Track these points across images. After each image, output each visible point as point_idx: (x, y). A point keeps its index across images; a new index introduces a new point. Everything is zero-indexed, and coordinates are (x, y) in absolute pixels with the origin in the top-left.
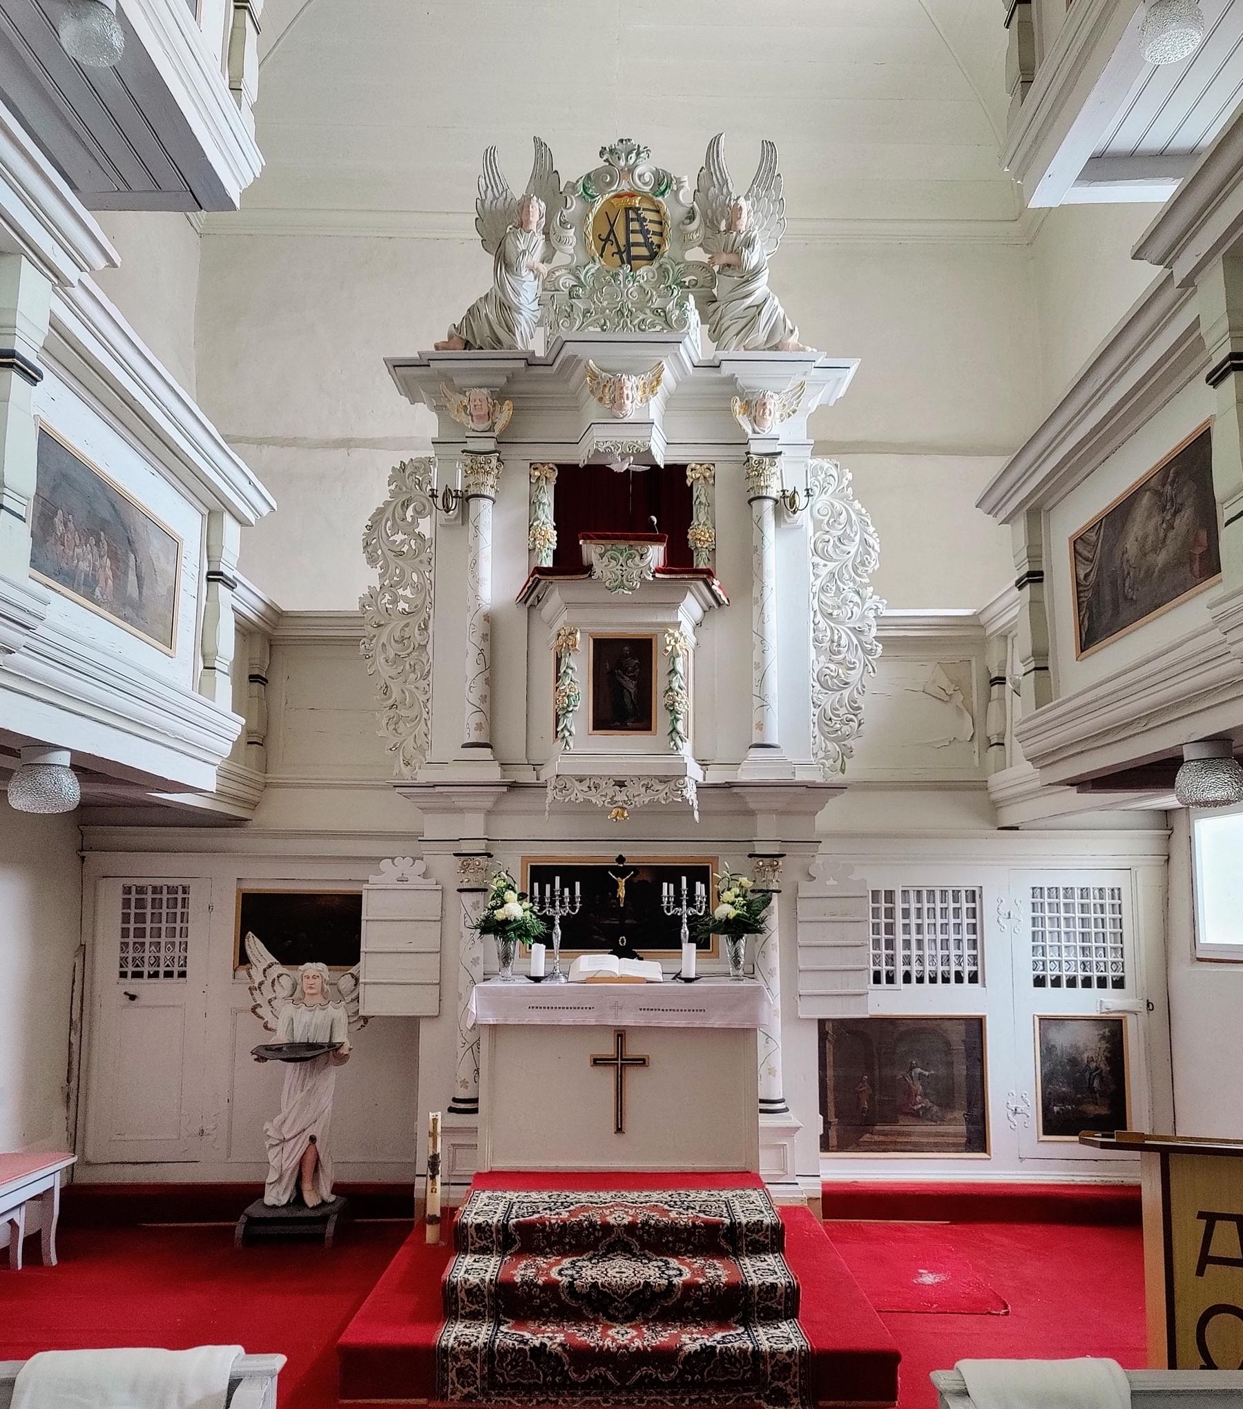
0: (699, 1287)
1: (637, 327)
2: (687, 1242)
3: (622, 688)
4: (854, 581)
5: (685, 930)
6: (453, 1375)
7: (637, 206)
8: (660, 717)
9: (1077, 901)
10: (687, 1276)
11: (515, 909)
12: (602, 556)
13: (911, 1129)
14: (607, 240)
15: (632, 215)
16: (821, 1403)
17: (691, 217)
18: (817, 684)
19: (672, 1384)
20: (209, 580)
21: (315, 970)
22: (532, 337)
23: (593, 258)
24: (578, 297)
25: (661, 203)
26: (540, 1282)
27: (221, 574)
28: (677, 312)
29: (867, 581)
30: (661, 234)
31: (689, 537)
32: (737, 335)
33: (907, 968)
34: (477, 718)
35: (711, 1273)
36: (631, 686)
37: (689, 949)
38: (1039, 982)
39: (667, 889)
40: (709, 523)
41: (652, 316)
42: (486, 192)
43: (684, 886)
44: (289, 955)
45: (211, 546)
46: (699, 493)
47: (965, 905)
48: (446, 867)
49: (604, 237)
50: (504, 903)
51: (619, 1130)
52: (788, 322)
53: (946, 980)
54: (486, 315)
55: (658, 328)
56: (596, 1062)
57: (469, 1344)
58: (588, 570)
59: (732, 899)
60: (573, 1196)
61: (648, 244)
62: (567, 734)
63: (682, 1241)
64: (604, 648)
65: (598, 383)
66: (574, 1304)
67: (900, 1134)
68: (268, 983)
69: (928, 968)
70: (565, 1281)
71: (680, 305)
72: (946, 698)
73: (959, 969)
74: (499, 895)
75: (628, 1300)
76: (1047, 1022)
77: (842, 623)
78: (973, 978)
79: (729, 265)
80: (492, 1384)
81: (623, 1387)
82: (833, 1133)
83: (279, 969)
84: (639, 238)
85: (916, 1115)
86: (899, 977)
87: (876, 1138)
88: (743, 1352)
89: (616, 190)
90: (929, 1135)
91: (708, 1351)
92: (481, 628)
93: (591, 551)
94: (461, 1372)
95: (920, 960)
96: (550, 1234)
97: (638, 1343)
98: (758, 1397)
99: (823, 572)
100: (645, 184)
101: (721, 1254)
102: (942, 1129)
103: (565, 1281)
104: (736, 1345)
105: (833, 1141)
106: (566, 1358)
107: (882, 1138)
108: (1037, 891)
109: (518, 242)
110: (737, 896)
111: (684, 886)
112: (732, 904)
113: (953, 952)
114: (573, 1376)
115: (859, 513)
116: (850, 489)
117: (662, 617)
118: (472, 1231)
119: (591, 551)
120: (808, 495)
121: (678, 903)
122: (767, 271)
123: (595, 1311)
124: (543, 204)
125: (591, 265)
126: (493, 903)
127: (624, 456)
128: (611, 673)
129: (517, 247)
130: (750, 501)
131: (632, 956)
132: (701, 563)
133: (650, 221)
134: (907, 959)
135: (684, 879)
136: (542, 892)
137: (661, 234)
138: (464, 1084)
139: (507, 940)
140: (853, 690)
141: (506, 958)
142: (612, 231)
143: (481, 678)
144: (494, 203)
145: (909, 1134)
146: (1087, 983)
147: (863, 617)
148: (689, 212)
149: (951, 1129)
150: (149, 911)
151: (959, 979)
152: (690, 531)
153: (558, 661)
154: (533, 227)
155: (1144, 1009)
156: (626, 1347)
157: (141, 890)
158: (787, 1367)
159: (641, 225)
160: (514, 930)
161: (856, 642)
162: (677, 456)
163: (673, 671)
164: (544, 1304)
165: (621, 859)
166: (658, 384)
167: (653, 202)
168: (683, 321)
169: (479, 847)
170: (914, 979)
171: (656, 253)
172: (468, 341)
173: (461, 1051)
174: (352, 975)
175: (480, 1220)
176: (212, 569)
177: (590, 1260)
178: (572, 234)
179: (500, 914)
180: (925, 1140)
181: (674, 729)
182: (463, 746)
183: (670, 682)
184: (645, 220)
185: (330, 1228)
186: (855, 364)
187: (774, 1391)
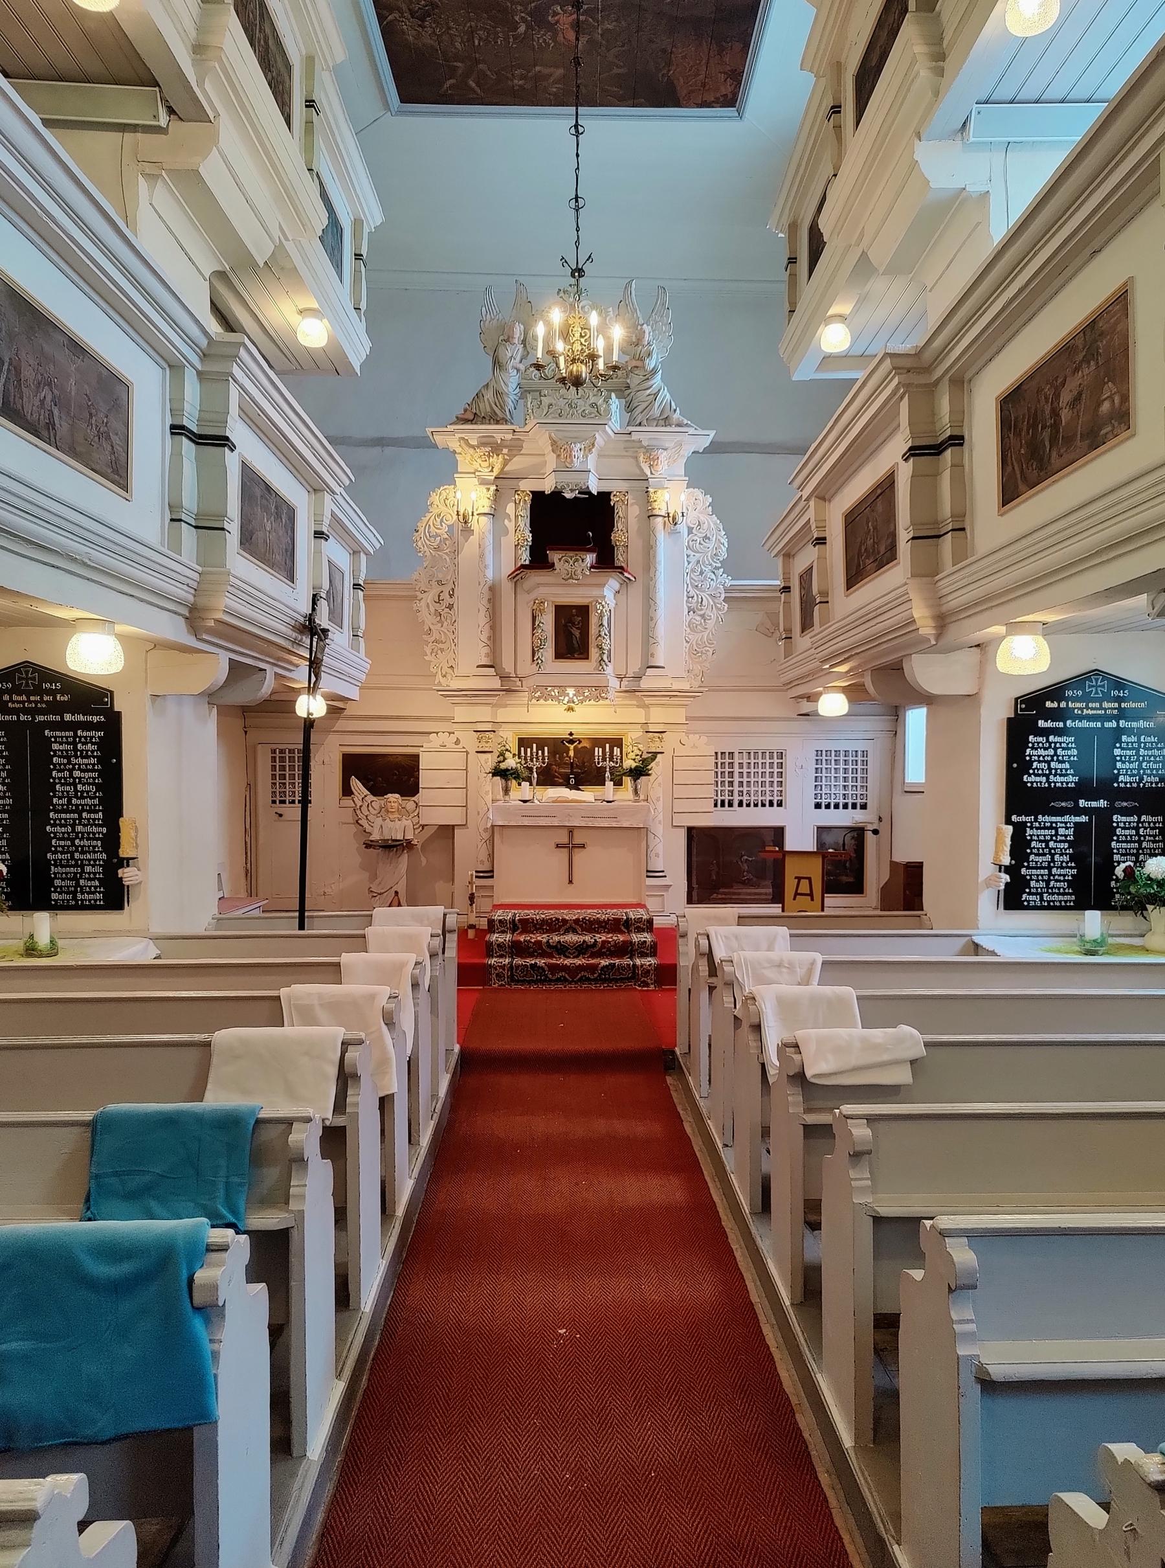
0: (609, 942)
2: (605, 928)
3: (570, 635)
5: (608, 774)
6: (494, 976)
8: (594, 652)
9: (842, 758)
10: (604, 938)
11: (511, 763)
12: (560, 560)
13: (740, 891)
18: (688, 629)
19: (595, 980)
20: (354, 588)
21: (393, 797)
22: (515, 409)
26: (533, 941)
27: (360, 585)
29: (720, 565)
31: (612, 538)
32: (642, 412)
33: (741, 798)
34: (486, 650)
35: (615, 938)
36: (577, 633)
37: (609, 784)
38: (818, 806)
39: (598, 752)
42: (486, 316)
43: (607, 750)
44: (377, 790)
45: (355, 573)
46: (620, 511)
47: (776, 761)
48: (470, 741)
50: (505, 759)
51: (571, 882)
53: (763, 805)
54: (488, 399)
55: (593, 415)
56: (558, 846)
58: (551, 566)
59: (634, 757)
60: (546, 912)
62: (540, 662)
63: (602, 927)
64: (560, 610)
66: (548, 950)
67: (735, 894)
69: (753, 798)
71: (606, 401)
72: (770, 635)
73: (772, 798)
74: (502, 754)
75: (575, 949)
76: (821, 830)
77: (704, 591)
78: (780, 804)
79: (637, 367)
80: (512, 979)
81: (573, 981)
82: (695, 894)
83: (371, 798)
85: (743, 883)
86: (736, 803)
87: (720, 896)
90: (750, 894)
92: (487, 595)
93: (554, 556)
94: (497, 975)
95: (749, 793)
96: (536, 924)
98: (635, 985)
99: (693, 560)
101: (622, 932)
103: (545, 940)
105: (695, 898)
106: (546, 968)
107: (723, 896)
108: (819, 753)
111: (607, 750)
112: (634, 760)
113: (768, 788)
115: (715, 524)
116: (710, 508)
117: (595, 592)
118: (497, 923)
119: (554, 556)
120: (683, 516)
121: (604, 760)
122: (660, 372)
123: (559, 954)
124: (522, 327)
126: (499, 759)
127: (572, 490)
128: (565, 626)
129: (506, 355)
130: (649, 517)
131: (579, 789)
132: (620, 559)
134: (741, 793)
135: (607, 745)
136: (526, 753)
138: (482, 862)
139: (507, 780)
141: (506, 791)
143: (487, 627)
145: (739, 894)
146: (845, 806)
150: (287, 764)
151: (771, 804)
152: (613, 535)
153: (534, 618)
155: (877, 821)
157: (282, 751)
158: (648, 971)
160: (511, 774)
161: (712, 603)
162: (605, 487)
163: (602, 625)
164: (535, 951)
165: (571, 734)
166: (593, 447)
168: (608, 411)
169: (488, 727)
170: (745, 805)
172: (475, 414)
174: (415, 802)
175: (501, 918)
176: (356, 582)
179: (503, 766)
180: (749, 897)
181: (602, 659)
182: (478, 667)
183: (600, 631)
186: (712, 433)
187: (642, 982)
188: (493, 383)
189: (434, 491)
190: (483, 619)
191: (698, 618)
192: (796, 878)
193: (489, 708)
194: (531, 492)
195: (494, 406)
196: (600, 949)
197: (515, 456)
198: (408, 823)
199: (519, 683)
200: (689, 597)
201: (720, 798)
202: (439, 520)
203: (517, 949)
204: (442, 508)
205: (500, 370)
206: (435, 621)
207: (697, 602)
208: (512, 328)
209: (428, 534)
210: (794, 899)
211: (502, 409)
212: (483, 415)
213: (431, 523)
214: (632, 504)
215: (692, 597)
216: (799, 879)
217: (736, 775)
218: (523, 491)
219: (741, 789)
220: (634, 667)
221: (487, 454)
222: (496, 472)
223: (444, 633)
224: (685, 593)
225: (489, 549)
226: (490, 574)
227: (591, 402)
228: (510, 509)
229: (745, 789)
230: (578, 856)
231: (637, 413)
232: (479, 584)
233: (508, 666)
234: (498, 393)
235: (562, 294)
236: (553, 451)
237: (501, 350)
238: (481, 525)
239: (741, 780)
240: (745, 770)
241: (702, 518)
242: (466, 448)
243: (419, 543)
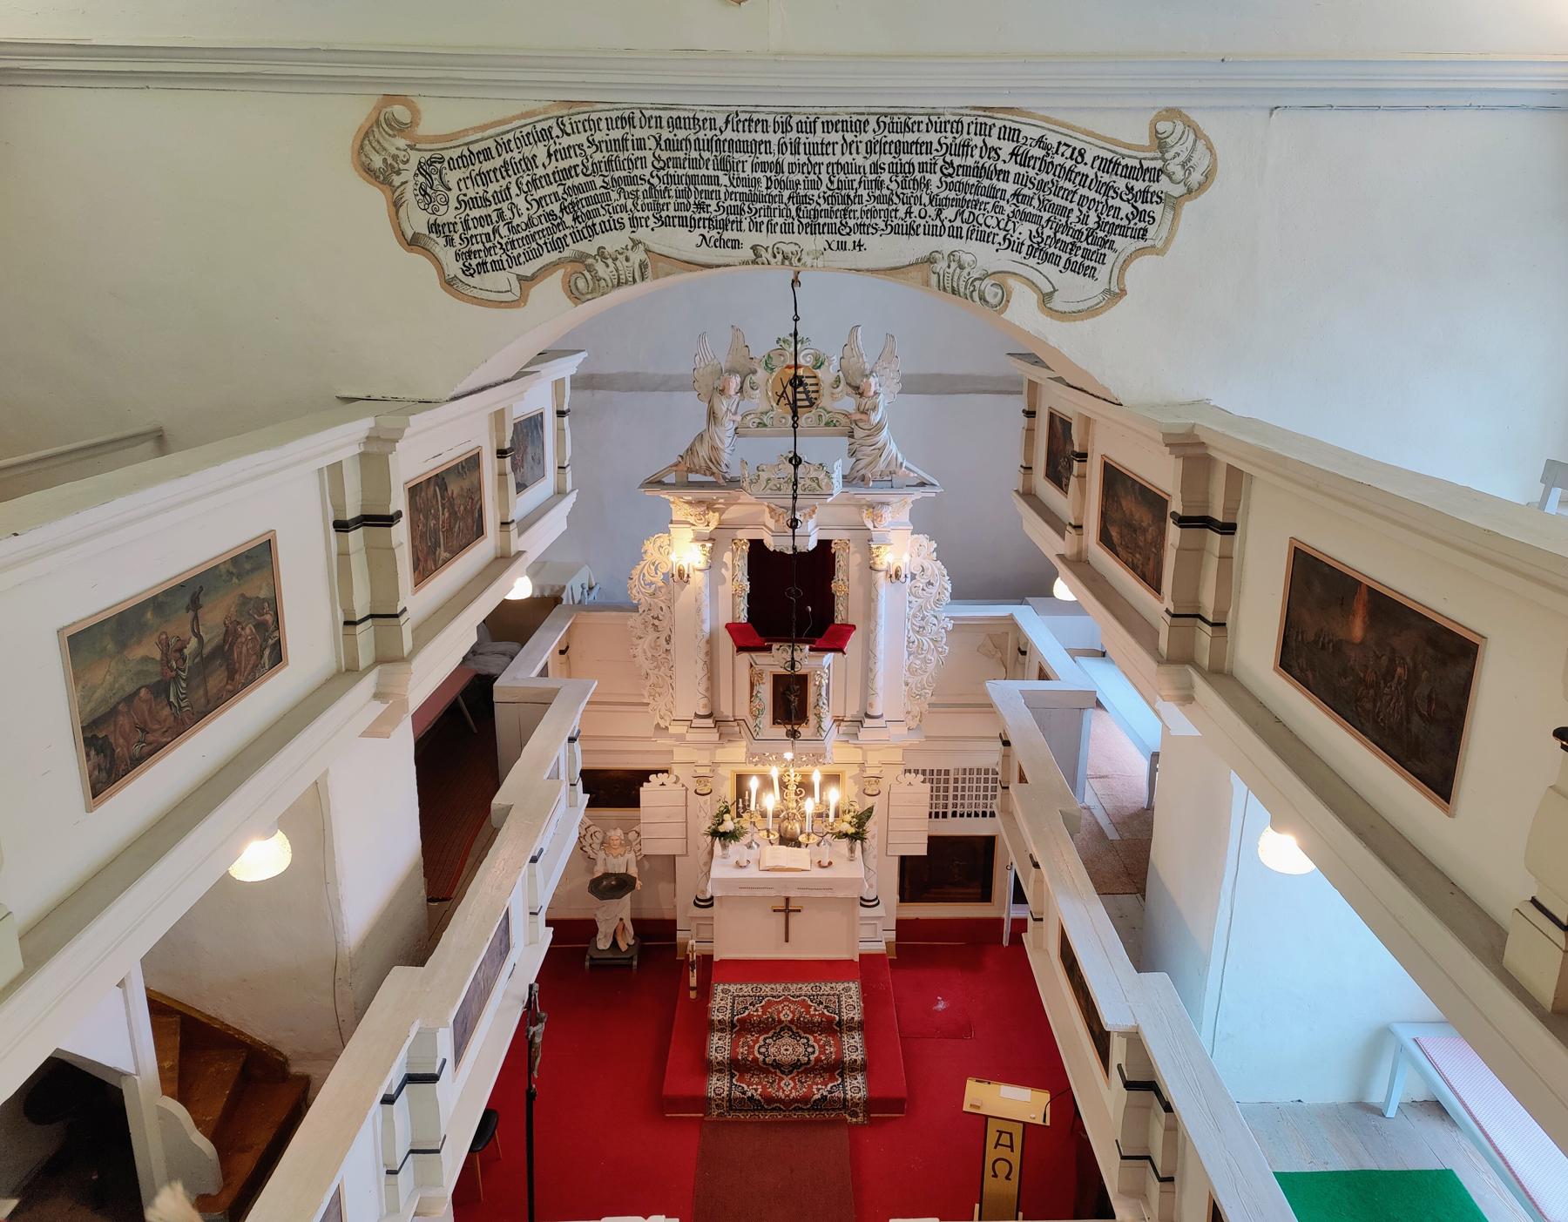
0: (822, 1061)
4: (934, 610)
12: (778, 649)
14: (781, 396)
16: (872, 1115)
17: (838, 380)
18: (908, 673)
19: (808, 1110)
24: (763, 470)
28: (826, 481)
30: (817, 384)
34: (704, 701)
40: (845, 578)
46: (840, 562)
52: (899, 456)
54: (703, 456)
57: (720, 1095)
61: (808, 399)
62: (758, 729)
68: (589, 835)
70: (761, 1058)
73: (984, 810)
80: (730, 1108)
84: (803, 396)
86: (950, 814)
88: (839, 1098)
91: (824, 1098)
92: (704, 648)
94: (717, 1105)
97: (794, 1094)
99: (915, 605)
100: (808, 362)
102: (968, 891)
104: (836, 1094)
106: (762, 1100)
110: (853, 817)
114: (766, 1107)
115: (939, 569)
116: (935, 553)
128: (784, 693)
129: (721, 409)
134: (955, 805)
140: (928, 677)
142: (784, 391)
143: (705, 679)
147: (938, 633)
149: (971, 891)
153: (752, 685)
154: (732, 392)
156: (788, 1096)
158: (858, 1104)
161: (933, 647)
162: (826, 536)
163: (820, 694)
170: (958, 815)
173: (700, 876)
177: (772, 1038)
179: (721, 829)
181: (820, 726)
184: (807, 384)
185: (635, 963)
188: (706, 438)
189: (648, 540)
190: (700, 671)
191: (918, 662)
192: (998, 1131)
193: (708, 752)
194: (750, 540)
195: (708, 461)
196: (815, 1065)
198: (631, 856)
199: (737, 729)
200: (909, 642)
201: (934, 810)
202: (653, 568)
203: (737, 1067)
204: (656, 555)
205: (715, 424)
206: (652, 666)
207: (918, 646)
208: (727, 381)
209: (642, 582)
210: (995, 1147)
213: (645, 571)
214: (853, 554)
215: (913, 642)
216: (1001, 1133)
217: (951, 789)
218: (741, 540)
219: (956, 793)
220: (853, 711)
222: (712, 527)
223: (662, 677)
224: (906, 638)
225: (706, 601)
226: (707, 628)
228: (727, 557)
229: (959, 802)
230: (793, 918)
231: (860, 467)
232: (696, 637)
233: (726, 710)
234: (714, 448)
235: (782, 343)
237: (716, 400)
238: (699, 580)
239: (956, 793)
240: (960, 785)
241: (926, 564)
243: (634, 591)
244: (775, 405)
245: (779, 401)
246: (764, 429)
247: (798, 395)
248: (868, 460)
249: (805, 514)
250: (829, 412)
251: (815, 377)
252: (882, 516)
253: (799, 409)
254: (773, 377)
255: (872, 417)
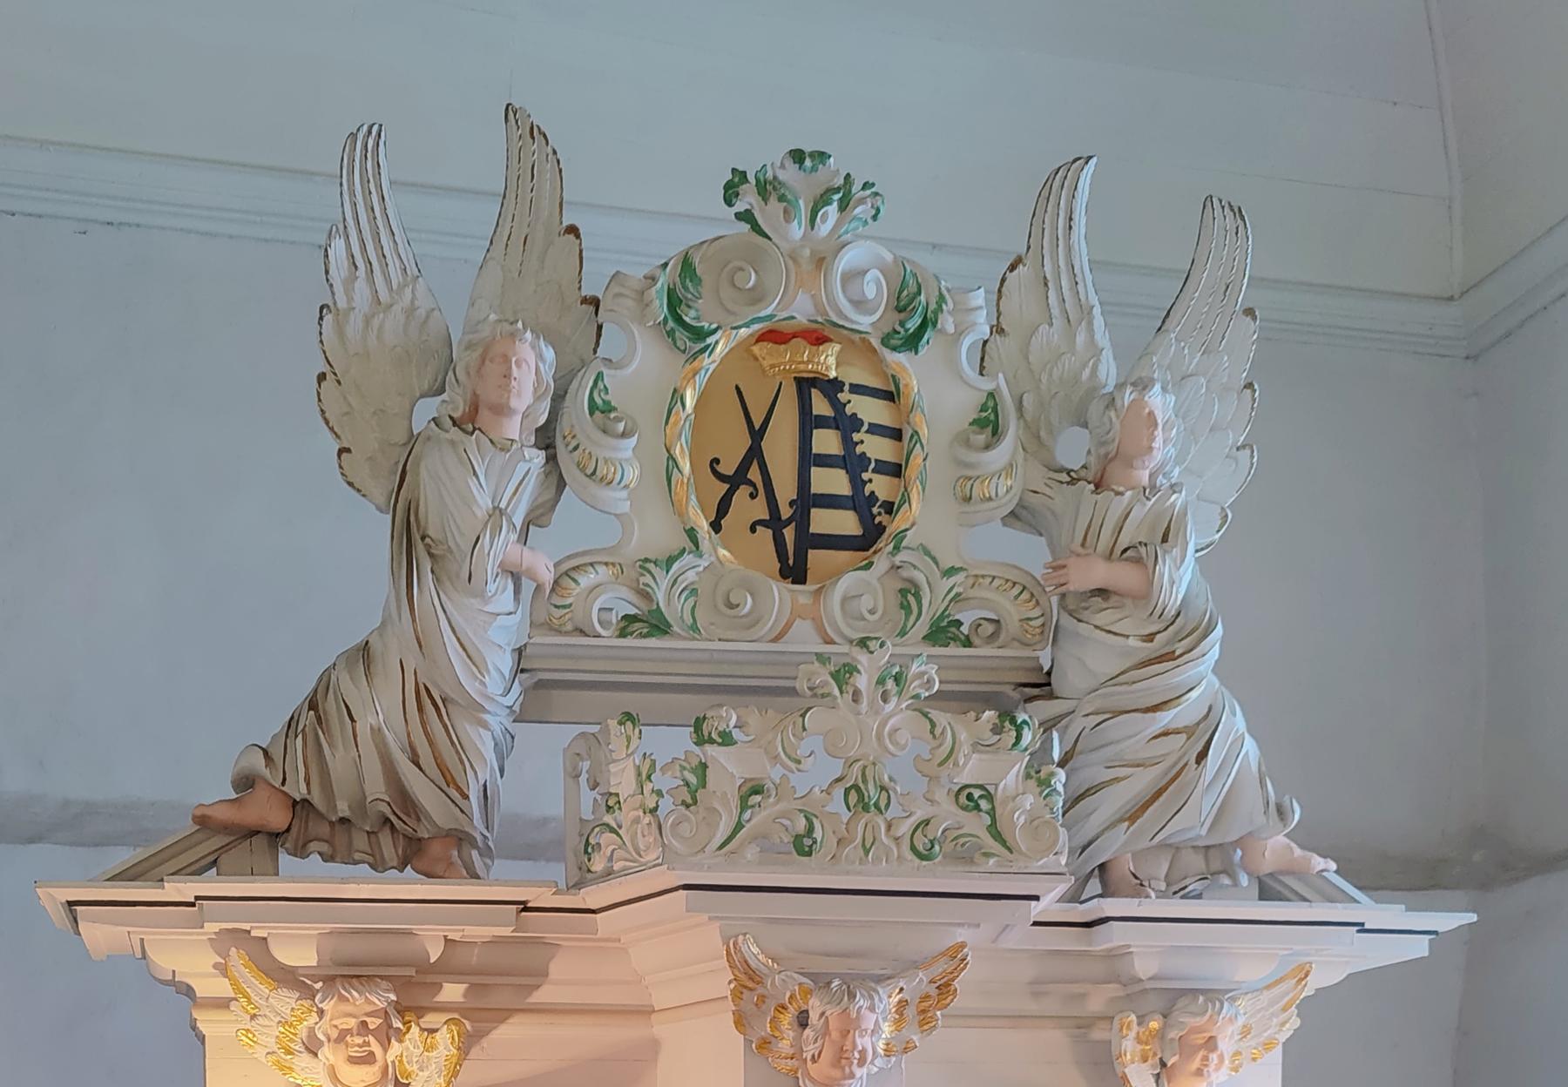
1: (906, 842)
7: (833, 374)
14: (736, 480)
15: (820, 406)
17: (989, 423)
23: (692, 534)
24: (726, 739)
25: (904, 369)
41: (954, 809)
49: (727, 469)
54: (376, 732)
61: (860, 502)
65: (762, 998)
89: (771, 317)
109: (473, 482)
125: (687, 559)
129: (468, 501)
133: (875, 429)
137: (895, 470)
142: (755, 453)
144: (376, 322)
148: (984, 408)
154: (513, 428)
159: (848, 443)
167: (878, 364)
171: (881, 529)
178: (629, 453)
184: (855, 423)
197: (503, 1015)
205: (438, 580)
211: (449, 782)
212: (343, 809)
221: (374, 1023)
227: (964, 779)
236: (740, 1022)
242: (258, 987)
244: (703, 525)
245: (723, 507)
246: (652, 642)
247: (816, 473)
248: (1141, 782)
249: (902, 1004)
250: (950, 572)
251: (890, 396)
252: (1211, 1043)
253: (813, 555)
254: (701, 379)
255: (1165, 569)
